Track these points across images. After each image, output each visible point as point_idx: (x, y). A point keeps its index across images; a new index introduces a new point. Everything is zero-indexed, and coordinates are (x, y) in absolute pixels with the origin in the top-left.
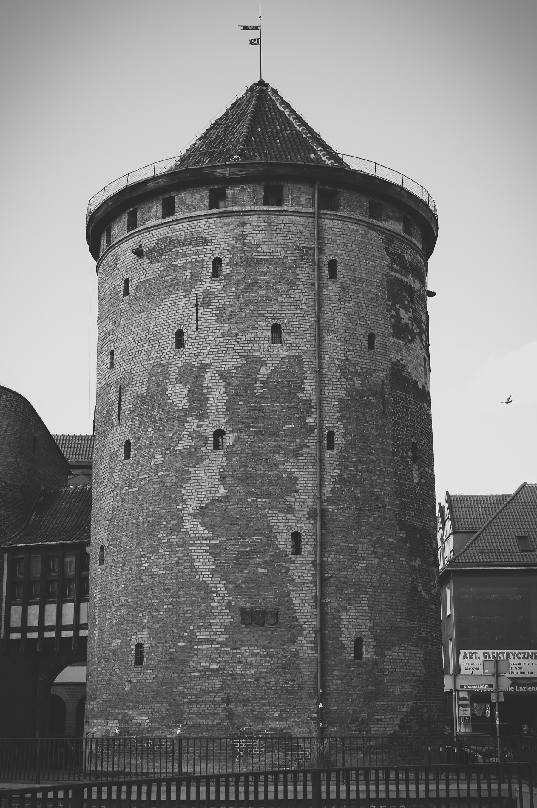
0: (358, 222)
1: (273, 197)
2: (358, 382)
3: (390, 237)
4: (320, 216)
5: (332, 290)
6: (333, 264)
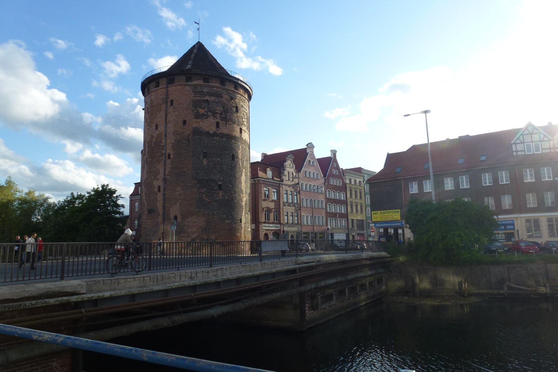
0: (181, 85)
1: (157, 86)
2: (178, 137)
3: (195, 86)
4: (167, 87)
5: (171, 109)
6: (172, 101)
